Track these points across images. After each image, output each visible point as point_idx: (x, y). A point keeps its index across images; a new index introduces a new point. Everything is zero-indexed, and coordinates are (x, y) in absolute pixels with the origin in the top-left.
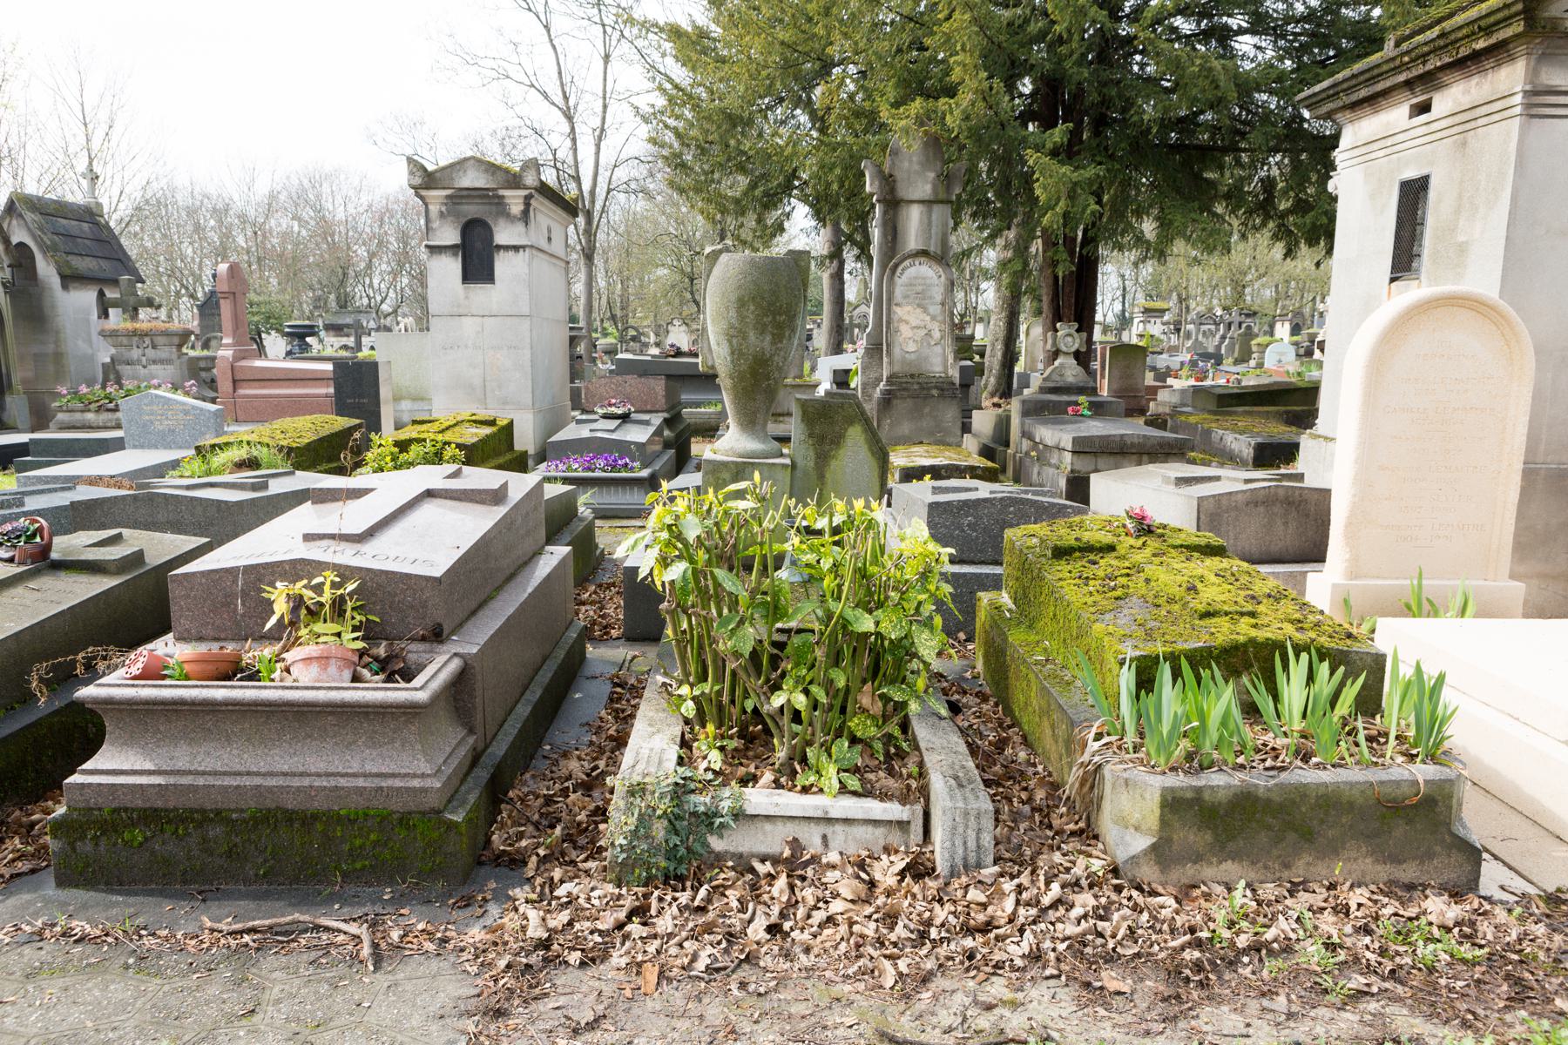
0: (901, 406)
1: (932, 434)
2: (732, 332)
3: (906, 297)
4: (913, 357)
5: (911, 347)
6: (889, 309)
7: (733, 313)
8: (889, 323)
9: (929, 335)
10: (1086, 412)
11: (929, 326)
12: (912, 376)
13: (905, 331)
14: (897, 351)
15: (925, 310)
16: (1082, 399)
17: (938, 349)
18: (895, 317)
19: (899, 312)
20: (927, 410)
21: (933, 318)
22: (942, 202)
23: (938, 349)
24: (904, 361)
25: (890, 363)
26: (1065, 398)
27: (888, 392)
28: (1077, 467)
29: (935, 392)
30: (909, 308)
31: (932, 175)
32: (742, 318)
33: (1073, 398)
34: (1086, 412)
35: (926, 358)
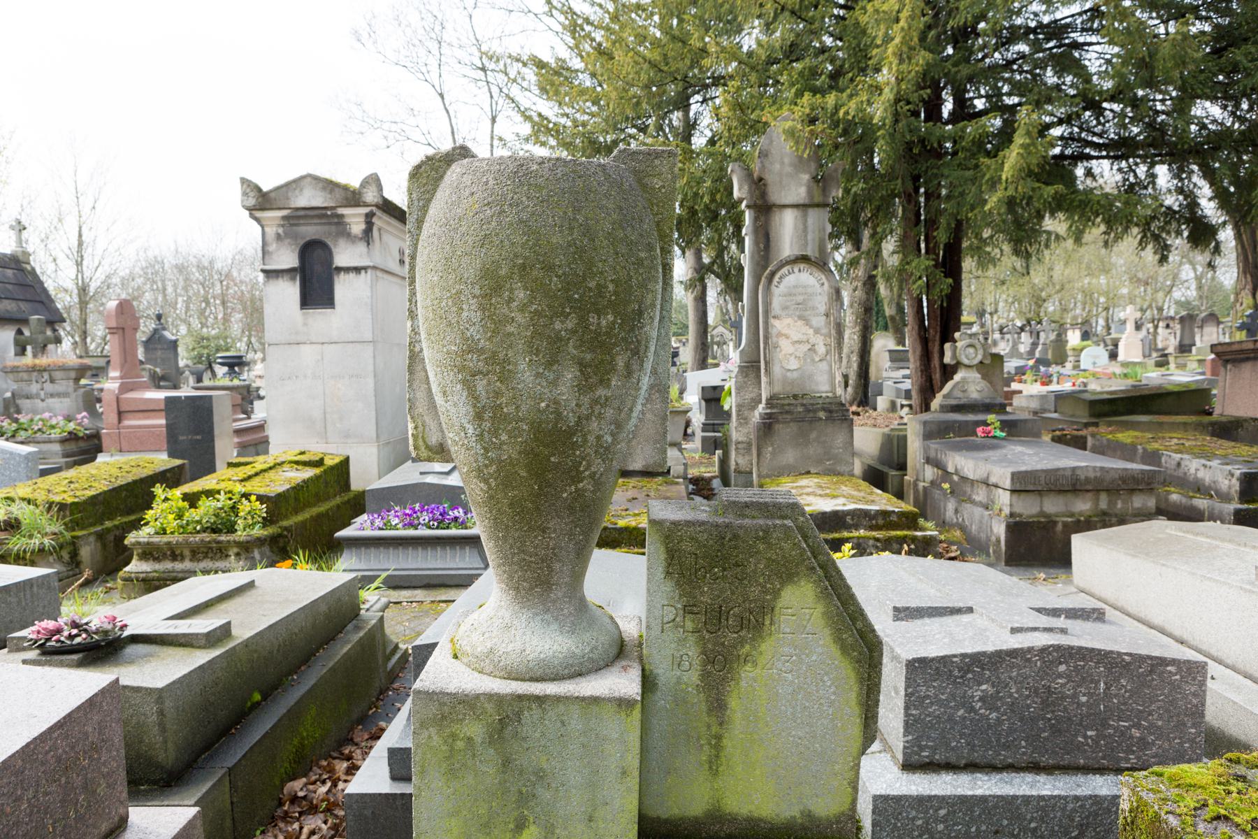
0: (784, 431)
1: (819, 462)
2: (473, 361)
3: (785, 308)
4: (795, 375)
5: (793, 364)
6: (766, 323)
7: (471, 312)
8: (766, 338)
9: (812, 349)
10: (999, 433)
11: (812, 340)
12: (795, 397)
13: (785, 347)
14: (776, 370)
15: (807, 322)
16: (991, 418)
17: (824, 366)
18: (773, 332)
19: (777, 325)
20: (813, 435)
21: (817, 331)
22: (817, 206)
23: (824, 366)
24: (785, 381)
25: (770, 383)
26: (971, 417)
27: (769, 416)
28: (1017, 510)
29: (822, 415)
30: (789, 320)
31: (806, 177)
32: (495, 323)
33: (980, 417)
34: (999, 433)
35: (810, 376)
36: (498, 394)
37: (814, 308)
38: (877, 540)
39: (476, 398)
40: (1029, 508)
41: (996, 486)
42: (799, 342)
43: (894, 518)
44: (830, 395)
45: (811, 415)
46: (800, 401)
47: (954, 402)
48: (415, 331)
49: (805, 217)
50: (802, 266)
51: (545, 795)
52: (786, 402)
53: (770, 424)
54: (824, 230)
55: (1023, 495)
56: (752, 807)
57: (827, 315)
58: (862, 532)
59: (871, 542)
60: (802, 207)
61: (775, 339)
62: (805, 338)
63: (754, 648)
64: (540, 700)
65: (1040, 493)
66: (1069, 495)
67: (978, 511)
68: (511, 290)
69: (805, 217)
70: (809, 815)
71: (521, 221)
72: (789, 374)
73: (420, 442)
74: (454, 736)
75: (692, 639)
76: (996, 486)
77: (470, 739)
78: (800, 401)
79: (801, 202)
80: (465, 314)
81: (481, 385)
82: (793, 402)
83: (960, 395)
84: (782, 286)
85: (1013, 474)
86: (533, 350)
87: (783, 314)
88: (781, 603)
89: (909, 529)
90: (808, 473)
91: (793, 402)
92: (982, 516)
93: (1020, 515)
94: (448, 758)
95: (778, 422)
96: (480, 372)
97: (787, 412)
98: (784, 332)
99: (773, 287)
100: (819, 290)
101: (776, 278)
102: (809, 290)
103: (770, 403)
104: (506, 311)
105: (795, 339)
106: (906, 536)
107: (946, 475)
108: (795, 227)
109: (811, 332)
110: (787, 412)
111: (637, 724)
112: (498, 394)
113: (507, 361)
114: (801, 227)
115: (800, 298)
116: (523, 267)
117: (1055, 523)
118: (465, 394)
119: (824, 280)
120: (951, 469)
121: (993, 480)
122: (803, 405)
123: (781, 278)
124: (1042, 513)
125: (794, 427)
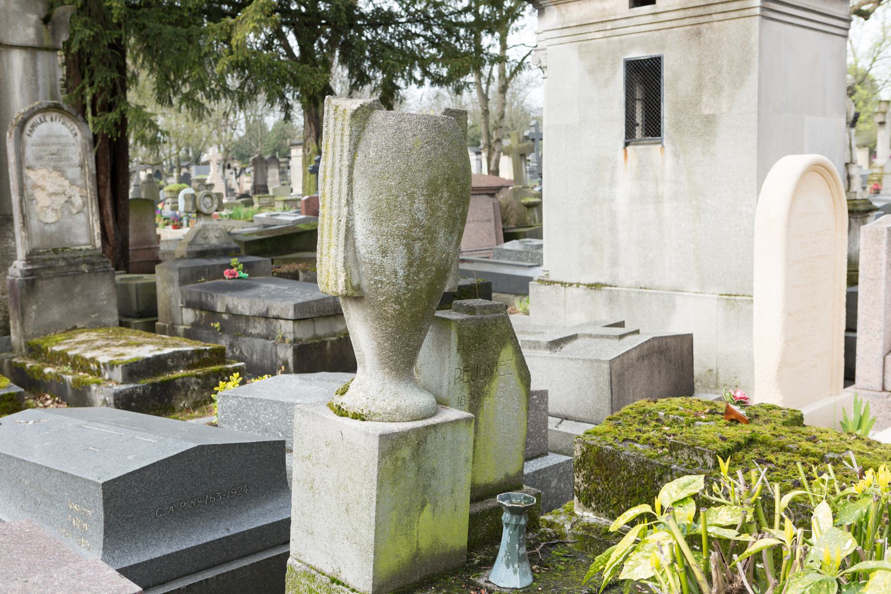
0: (48, 287)
1: (85, 316)
2: (417, 232)
3: (39, 158)
4: (53, 228)
5: (51, 217)
6: (20, 174)
7: (420, 204)
8: (22, 189)
9: (69, 201)
10: (242, 274)
11: (69, 192)
12: (55, 251)
13: (42, 199)
14: (34, 223)
15: (63, 174)
16: (234, 261)
17: (81, 218)
18: (28, 183)
19: (32, 176)
20: (78, 289)
21: (73, 183)
22: (47, 49)
23: (81, 218)
24: (43, 234)
25: (29, 237)
26: (215, 262)
27: (31, 272)
28: (298, 336)
29: (84, 268)
30: (43, 172)
31: (33, 18)
32: (432, 210)
33: (223, 261)
34: (242, 274)
35: (69, 229)
36: (426, 250)
37: (68, 159)
38: (198, 377)
39: (412, 254)
40: (306, 333)
41: (277, 318)
42: (55, 194)
43: (206, 356)
44: (89, 247)
45: (74, 269)
46: (61, 255)
47: (198, 249)
48: (350, 214)
49: (34, 60)
50: (54, 115)
51: (434, 483)
52: (47, 256)
53: (33, 281)
54: (55, 75)
55: (302, 322)
56: (486, 478)
57: (82, 166)
58: (182, 372)
59: (193, 380)
60: (31, 49)
61: (30, 191)
62: (60, 190)
63: (490, 386)
64: (435, 426)
65: (312, 319)
66: (332, 319)
67: (259, 343)
68: (442, 192)
69: (34, 60)
70: (507, 476)
71: (445, 154)
72: (47, 228)
73: (349, 285)
74: (397, 459)
75: (466, 385)
76: (277, 318)
77: (404, 459)
78: (61, 255)
79: (30, 43)
80: (416, 205)
81: (417, 246)
82: (54, 256)
83: (202, 241)
84: (34, 135)
85: (295, 306)
86: (447, 226)
87: (38, 164)
88: (500, 359)
89: (219, 363)
90: (75, 328)
91: (54, 256)
92: (265, 346)
93: (301, 340)
94: (393, 474)
95: (41, 278)
96: (419, 239)
97: (49, 268)
98: (39, 183)
99: (25, 137)
100: (72, 141)
101: (28, 127)
102: (63, 140)
103: (30, 258)
104: (438, 203)
105: (51, 190)
106: (221, 370)
107: (213, 313)
108: (25, 69)
109: (66, 183)
110: (49, 268)
111: (473, 431)
112: (426, 250)
113: (435, 232)
114: (31, 70)
115: (54, 149)
116: (448, 179)
117: (325, 342)
118: (405, 251)
119: (77, 130)
120: (220, 308)
121: (273, 313)
122: (64, 259)
123: (33, 126)
124: (315, 336)
125: (57, 282)
